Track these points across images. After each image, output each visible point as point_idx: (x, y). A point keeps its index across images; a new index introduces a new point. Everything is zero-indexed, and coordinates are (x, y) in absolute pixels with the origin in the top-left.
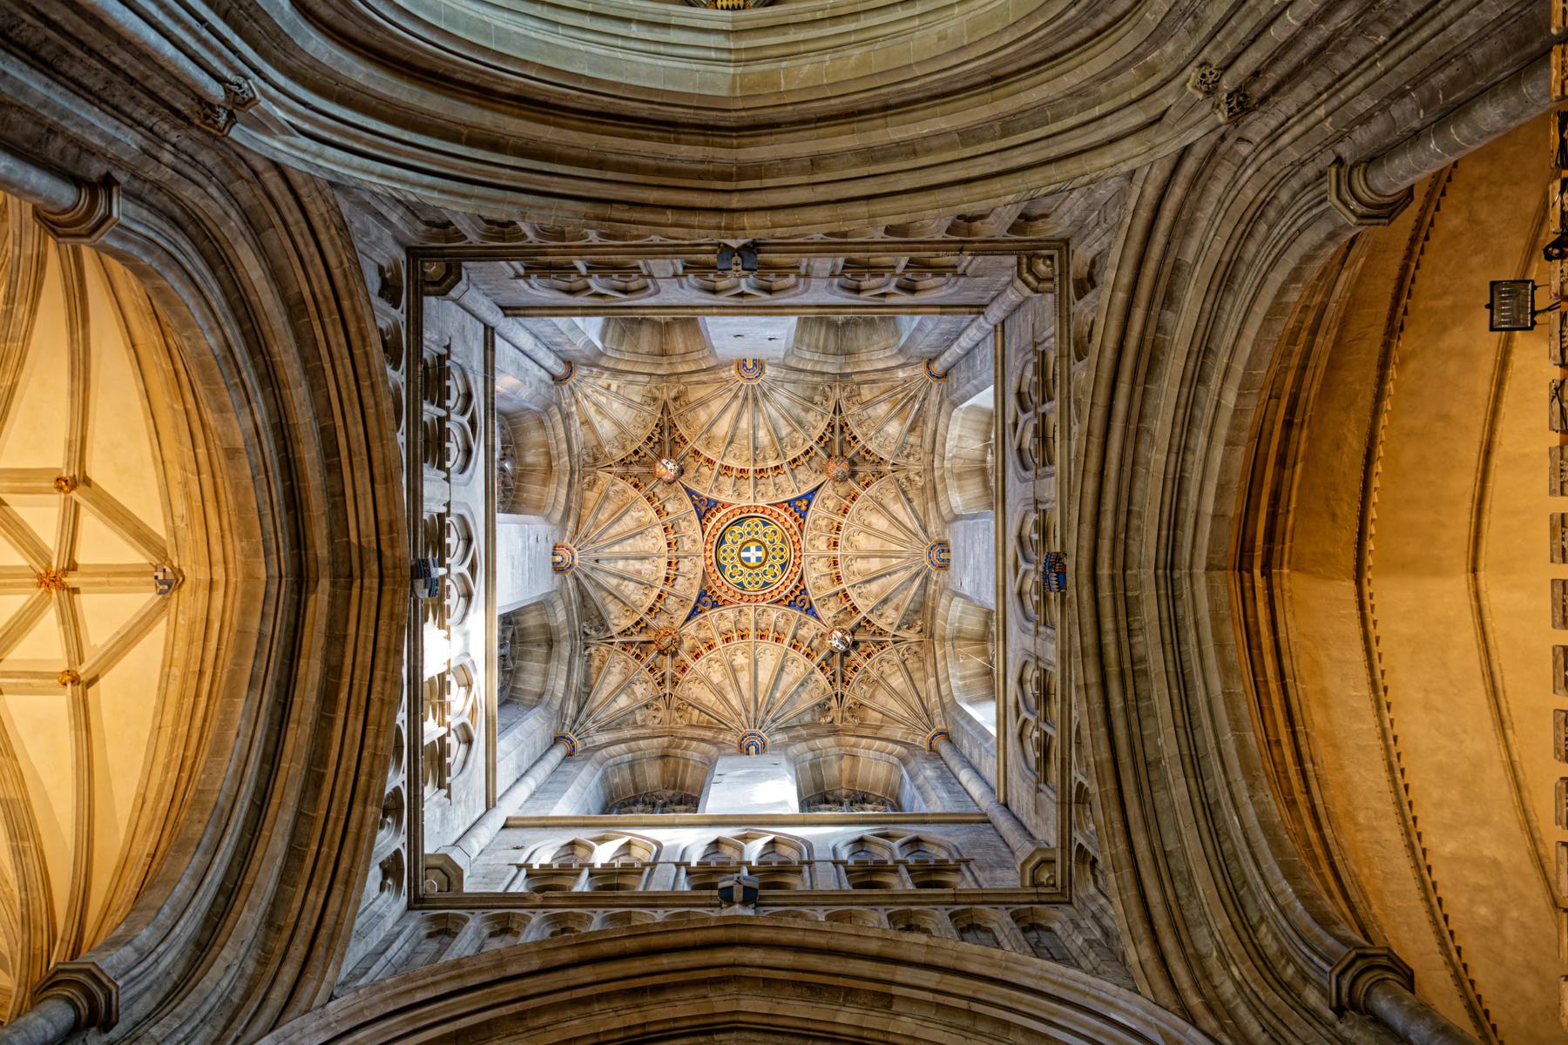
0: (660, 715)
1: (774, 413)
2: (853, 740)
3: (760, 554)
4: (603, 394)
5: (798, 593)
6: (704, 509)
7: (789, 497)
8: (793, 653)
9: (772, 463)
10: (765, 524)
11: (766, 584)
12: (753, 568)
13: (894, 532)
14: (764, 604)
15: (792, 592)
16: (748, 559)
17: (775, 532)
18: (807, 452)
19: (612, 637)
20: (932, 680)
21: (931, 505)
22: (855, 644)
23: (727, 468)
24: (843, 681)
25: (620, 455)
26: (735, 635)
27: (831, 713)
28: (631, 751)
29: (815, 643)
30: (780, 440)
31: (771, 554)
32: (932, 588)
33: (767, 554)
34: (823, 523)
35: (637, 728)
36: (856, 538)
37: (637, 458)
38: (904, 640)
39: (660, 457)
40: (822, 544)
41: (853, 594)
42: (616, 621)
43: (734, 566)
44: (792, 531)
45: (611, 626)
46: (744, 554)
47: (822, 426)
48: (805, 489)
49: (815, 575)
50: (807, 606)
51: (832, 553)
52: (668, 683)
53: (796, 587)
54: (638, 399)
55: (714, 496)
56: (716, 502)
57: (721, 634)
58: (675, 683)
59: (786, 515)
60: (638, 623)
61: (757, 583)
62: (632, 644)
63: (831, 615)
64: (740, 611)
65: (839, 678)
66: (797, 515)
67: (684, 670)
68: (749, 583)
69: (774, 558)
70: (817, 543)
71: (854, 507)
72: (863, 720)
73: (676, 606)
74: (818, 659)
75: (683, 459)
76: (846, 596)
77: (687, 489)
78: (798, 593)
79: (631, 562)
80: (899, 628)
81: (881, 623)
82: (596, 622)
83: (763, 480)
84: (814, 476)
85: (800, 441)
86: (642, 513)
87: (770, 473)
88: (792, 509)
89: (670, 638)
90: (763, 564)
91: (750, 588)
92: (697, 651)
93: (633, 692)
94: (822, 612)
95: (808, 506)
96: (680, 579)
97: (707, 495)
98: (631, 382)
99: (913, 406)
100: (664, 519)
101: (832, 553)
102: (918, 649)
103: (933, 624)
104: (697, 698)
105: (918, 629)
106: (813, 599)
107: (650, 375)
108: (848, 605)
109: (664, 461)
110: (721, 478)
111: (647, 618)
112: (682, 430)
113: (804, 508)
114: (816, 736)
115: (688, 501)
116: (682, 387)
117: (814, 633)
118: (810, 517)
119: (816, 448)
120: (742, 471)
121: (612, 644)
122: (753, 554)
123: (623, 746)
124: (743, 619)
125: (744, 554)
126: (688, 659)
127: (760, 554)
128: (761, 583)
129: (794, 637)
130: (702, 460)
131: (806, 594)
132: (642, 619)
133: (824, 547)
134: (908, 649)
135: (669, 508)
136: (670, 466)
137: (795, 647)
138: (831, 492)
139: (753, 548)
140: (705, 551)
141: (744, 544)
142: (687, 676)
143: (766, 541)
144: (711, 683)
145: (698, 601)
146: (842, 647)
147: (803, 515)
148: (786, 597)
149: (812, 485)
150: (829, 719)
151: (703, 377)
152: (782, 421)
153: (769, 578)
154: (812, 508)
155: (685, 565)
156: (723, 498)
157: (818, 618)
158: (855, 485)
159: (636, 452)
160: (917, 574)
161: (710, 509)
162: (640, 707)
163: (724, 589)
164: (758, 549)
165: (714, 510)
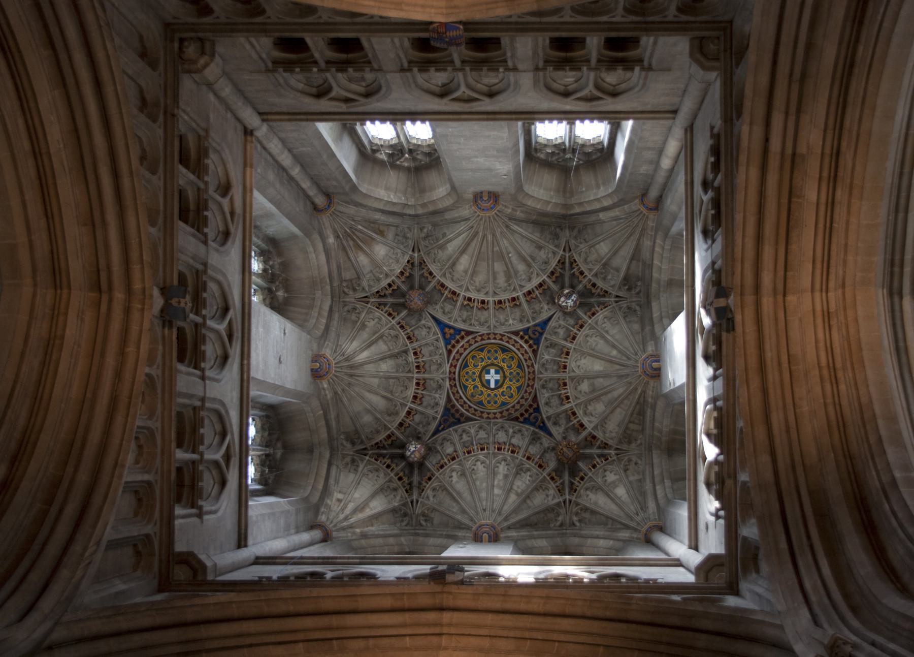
0: (634, 459)
1: (364, 355)
2: (654, 285)
3: (492, 371)
4: (345, 506)
5: (526, 337)
6: (452, 420)
7: (442, 343)
8: (580, 337)
9: (411, 358)
10: (466, 366)
11: (520, 366)
12: (505, 377)
13: (470, 250)
14: (536, 366)
15: (526, 342)
16: (497, 381)
17: (474, 357)
18: (402, 327)
19: (565, 502)
20: (602, 216)
21: (448, 216)
22: (572, 287)
23: (415, 397)
24: (604, 296)
25: (401, 492)
26: (563, 392)
27: (634, 305)
28: (663, 481)
29: (571, 321)
30: (390, 350)
31: (493, 360)
32: (519, 214)
33: (492, 365)
34: (465, 314)
35: (644, 479)
36: (477, 284)
37: (405, 479)
38: (567, 242)
39: (403, 457)
40: (483, 316)
41: (529, 287)
42: (550, 498)
43: (503, 394)
44: (472, 342)
45: (556, 501)
46: (492, 385)
47: (378, 313)
48: (435, 328)
49: (511, 322)
50: (539, 329)
51: (491, 305)
52: (606, 451)
53: (522, 338)
54: (352, 476)
55: (441, 410)
56: (446, 409)
57: (562, 404)
58: (605, 446)
59: (458, 347)
60: (552, 478)
61: (518, 374)
62: (572, 484)
63: (546, 307)
64: (543, 387)
65: (602, 299)
66: (458, 337)
67: (594, 437)
68: (518, 381)
69: (496, 358)
70: (482, 320)
71: (451, 286)
72: (638, 279)
73: (538, 445)
74: (586, 318)
75: (408, 437)
76: (529, 293)
77: (434, 434)
78: (526, 337)
79: (496, 483)
80: (557, 246)
81: (554, 263)
82: (551, 516)
83: (427, 366)
84: (423, 322)
85: (393, 332)
86: (454, 474)
87: (420, 360)
88: (453, 342)
89: (565, 449)
90: (502, 368)
91: (522, 380)
92: (577, 425)
93: (614, 482)
94: (544, 316)
95: (450, 327)
96: (514, 441)
97: (439, 417)
98: (337, 481)
99: (360, 231)
100: (460, 453)
101: (491, 305)
102: (576, 230)
103: (552, 215)
104: (619, 425)
105: (558, 230)
106: (532, 323)
107: (330, 465)
108: (537, 292)
109: (408, 453)
110: (425, 404)
111: (548, 470)
112: (382, 436)
113: (452, 331)
114: (651, 319)
115: (443, 434)
116: (342, 437)
117: (562, 322)
118: (460, 325)
119: (397, 319)
120: (418, 384)
121: (570, 501)
122: (492, 377)
123: (658, 487)
124: (550, 385)
125: (492, 385)
126: (584, 434)
127: (492, 371)
128: (518, 370)
129: (566, 340)
130: (408, 421)
131: (528, 329)
132: (549, 475)
133: (485, 313)
134: (576, 238)
135: (450, 450)
136: (412, 448)
137: (574, 338)
138: (438, 307)
139: (487, 377)
140: (488, 418)
141: (483, 385)
142: (599, 434)
143: (481, 365)
144: (604, 412)
145: (533, 424)
146: (574, 297)
147: (458, 331)
148: (530, 346)
149: (431, 323)
150: (638, 308)
151: (332, 415)
152: (373, 348)
153: (514, 364)
154: (452, 324)
155: (501, 437)
156: (443, 402)
157: (550, 318)
158: (431, 285)
159: (400, 479)
160: (507, 227)
161: (453, 415)
162: (627, 476)
163: (523, 402)
164: (488, 372)
165: (453, 411)
